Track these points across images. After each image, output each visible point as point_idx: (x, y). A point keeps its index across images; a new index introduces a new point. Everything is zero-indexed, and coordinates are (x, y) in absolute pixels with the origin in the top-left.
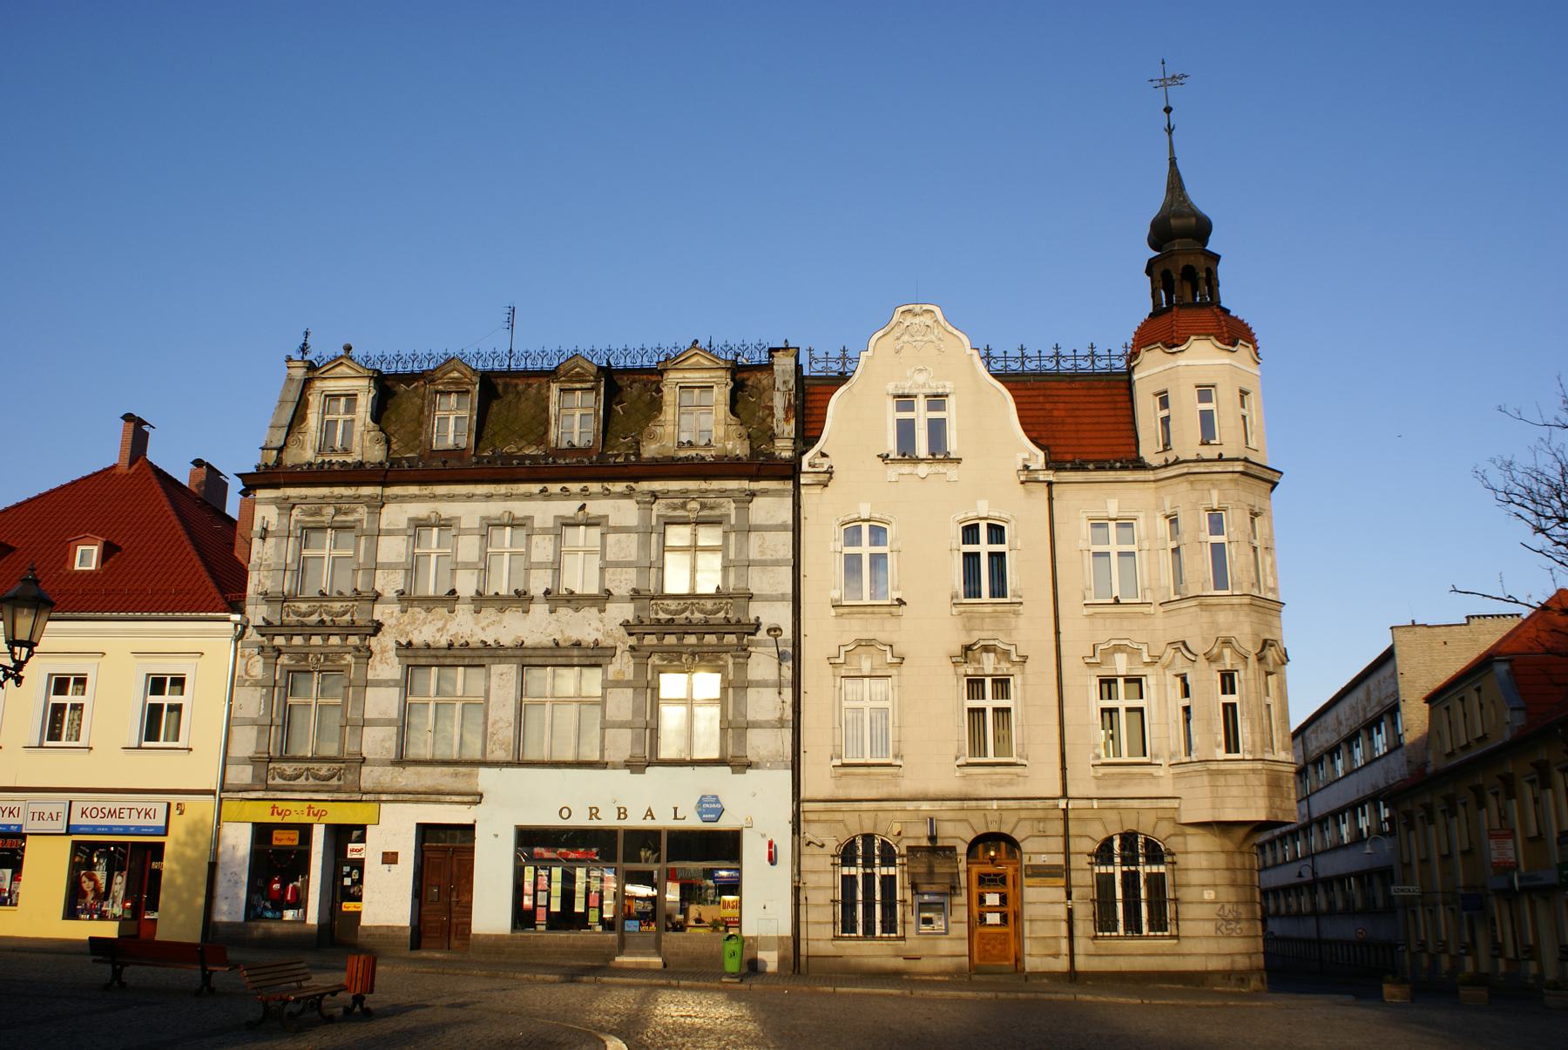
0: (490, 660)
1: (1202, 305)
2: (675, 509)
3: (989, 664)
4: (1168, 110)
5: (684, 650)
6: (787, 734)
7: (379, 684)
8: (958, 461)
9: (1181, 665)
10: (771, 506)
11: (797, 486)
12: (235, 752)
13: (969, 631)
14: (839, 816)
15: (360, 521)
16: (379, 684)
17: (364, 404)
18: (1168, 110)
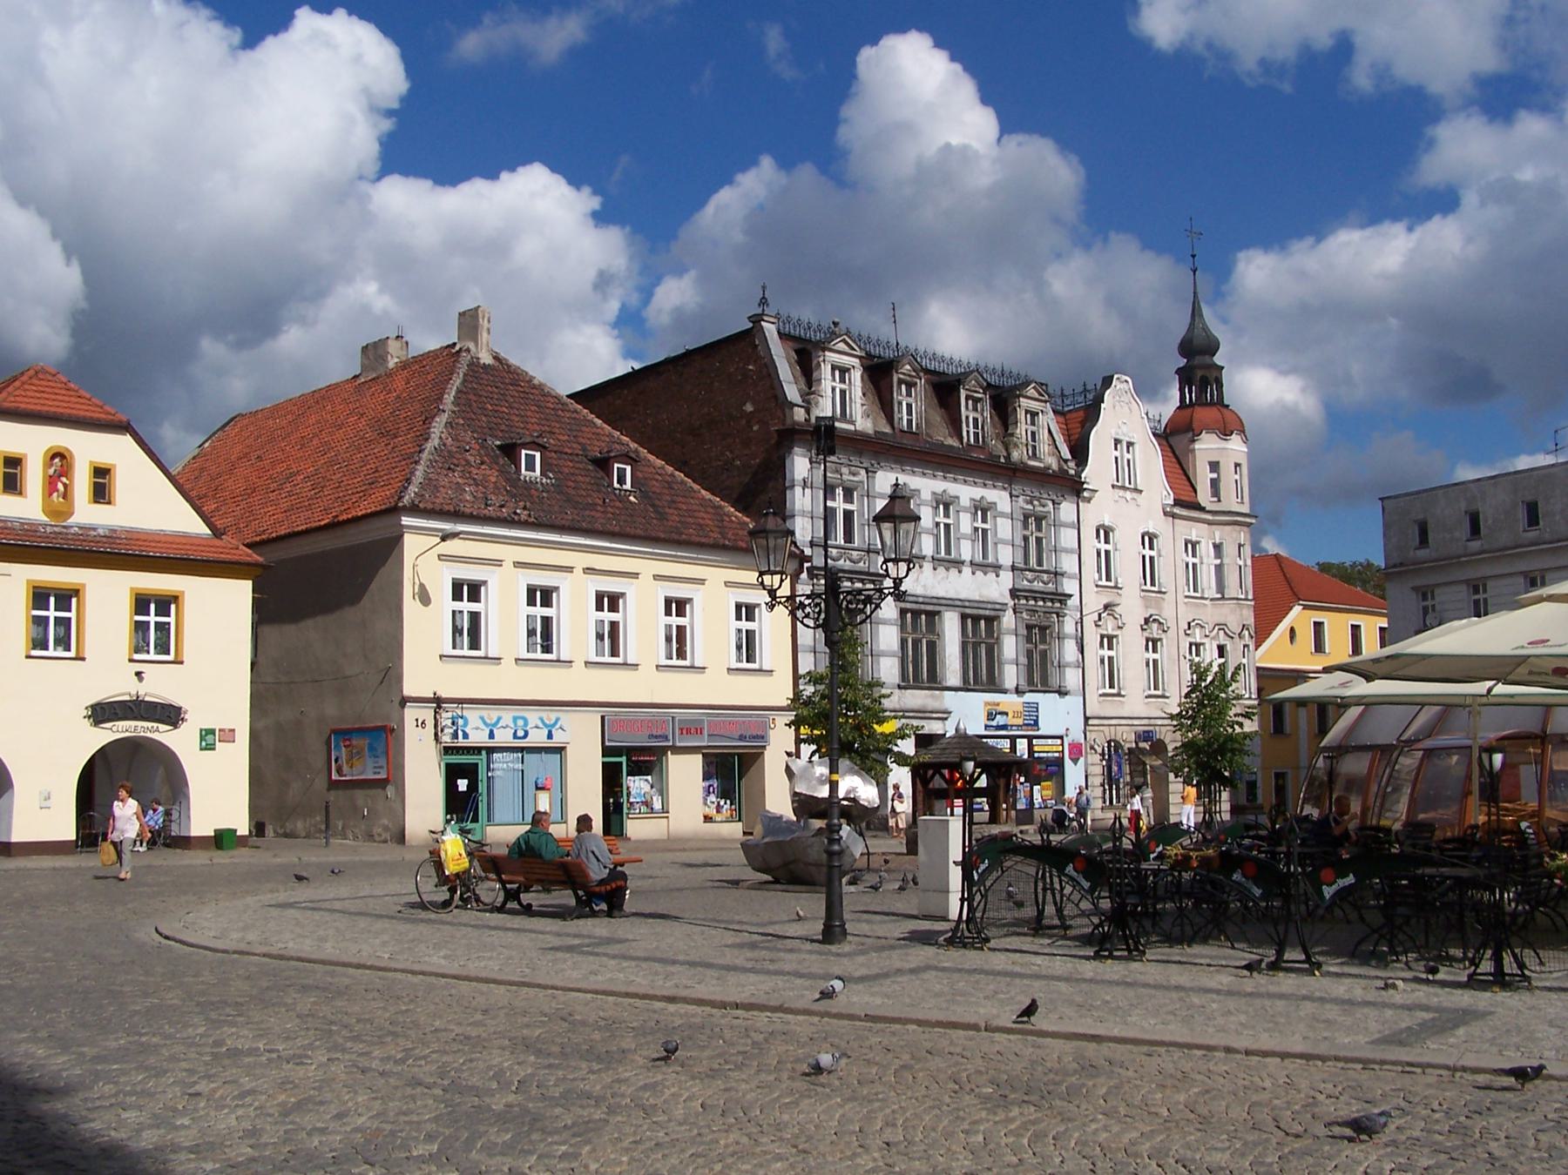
0: (945, 608)
1: (1212, 404)
2: (1027, 503)
3: (1155, 630)
4: (1193, 256)
5: (1038, 609)
6: (1081, 670)
7: (885, 622)
8: (1141, 491)
9: (1223, 640)
10: (1067, 510)
11: (1078, 497)
12: (802, 671)
13: (1147, 607)
14: (1101, 728)
15: (862, 482)
16: (885, 622)
17: (857, 376)
18: (1193, 256)
